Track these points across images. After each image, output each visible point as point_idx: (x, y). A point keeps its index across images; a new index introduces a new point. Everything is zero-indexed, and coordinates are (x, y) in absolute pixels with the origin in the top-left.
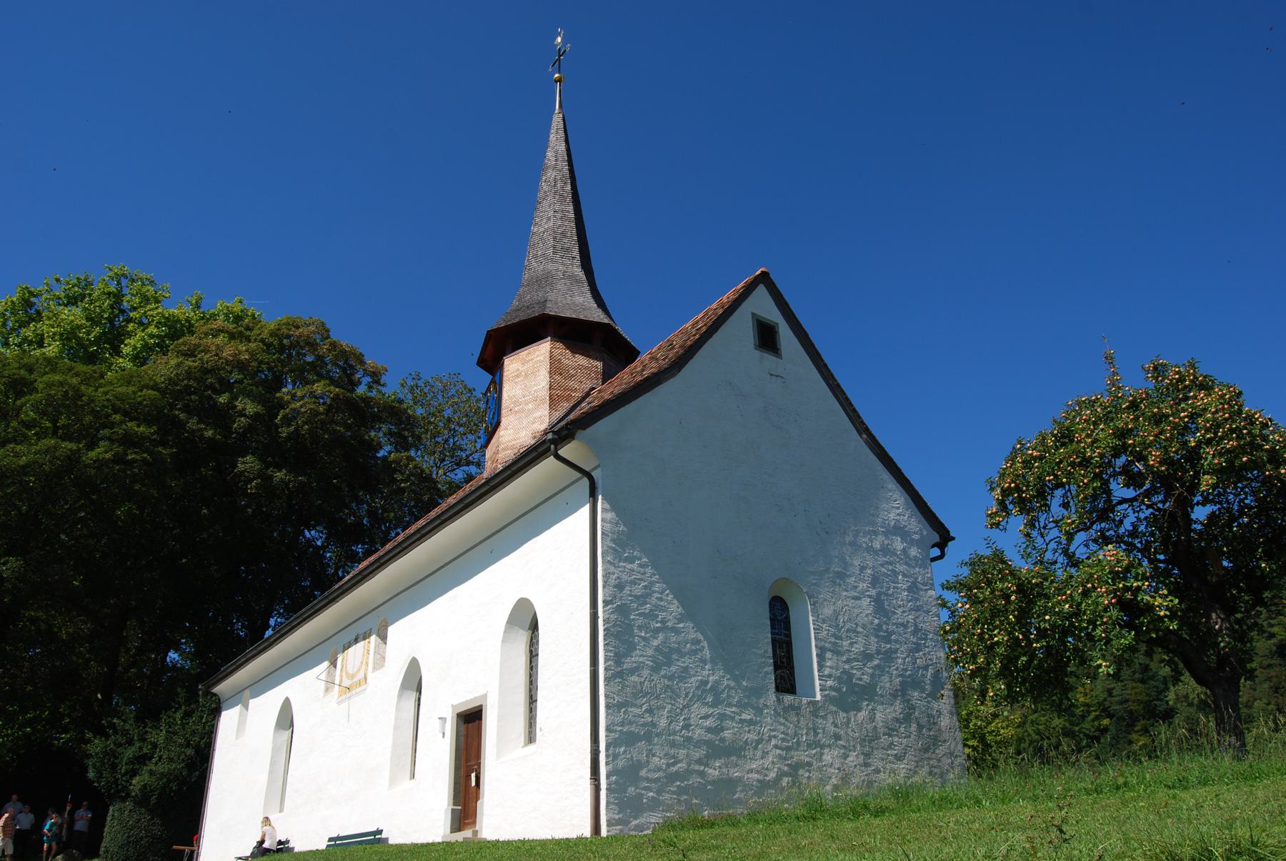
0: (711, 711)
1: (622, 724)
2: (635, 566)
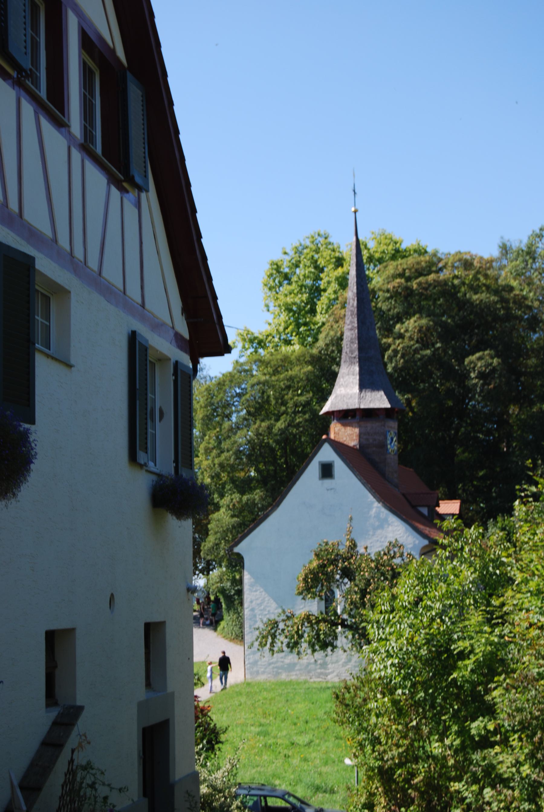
2: (258, 593)
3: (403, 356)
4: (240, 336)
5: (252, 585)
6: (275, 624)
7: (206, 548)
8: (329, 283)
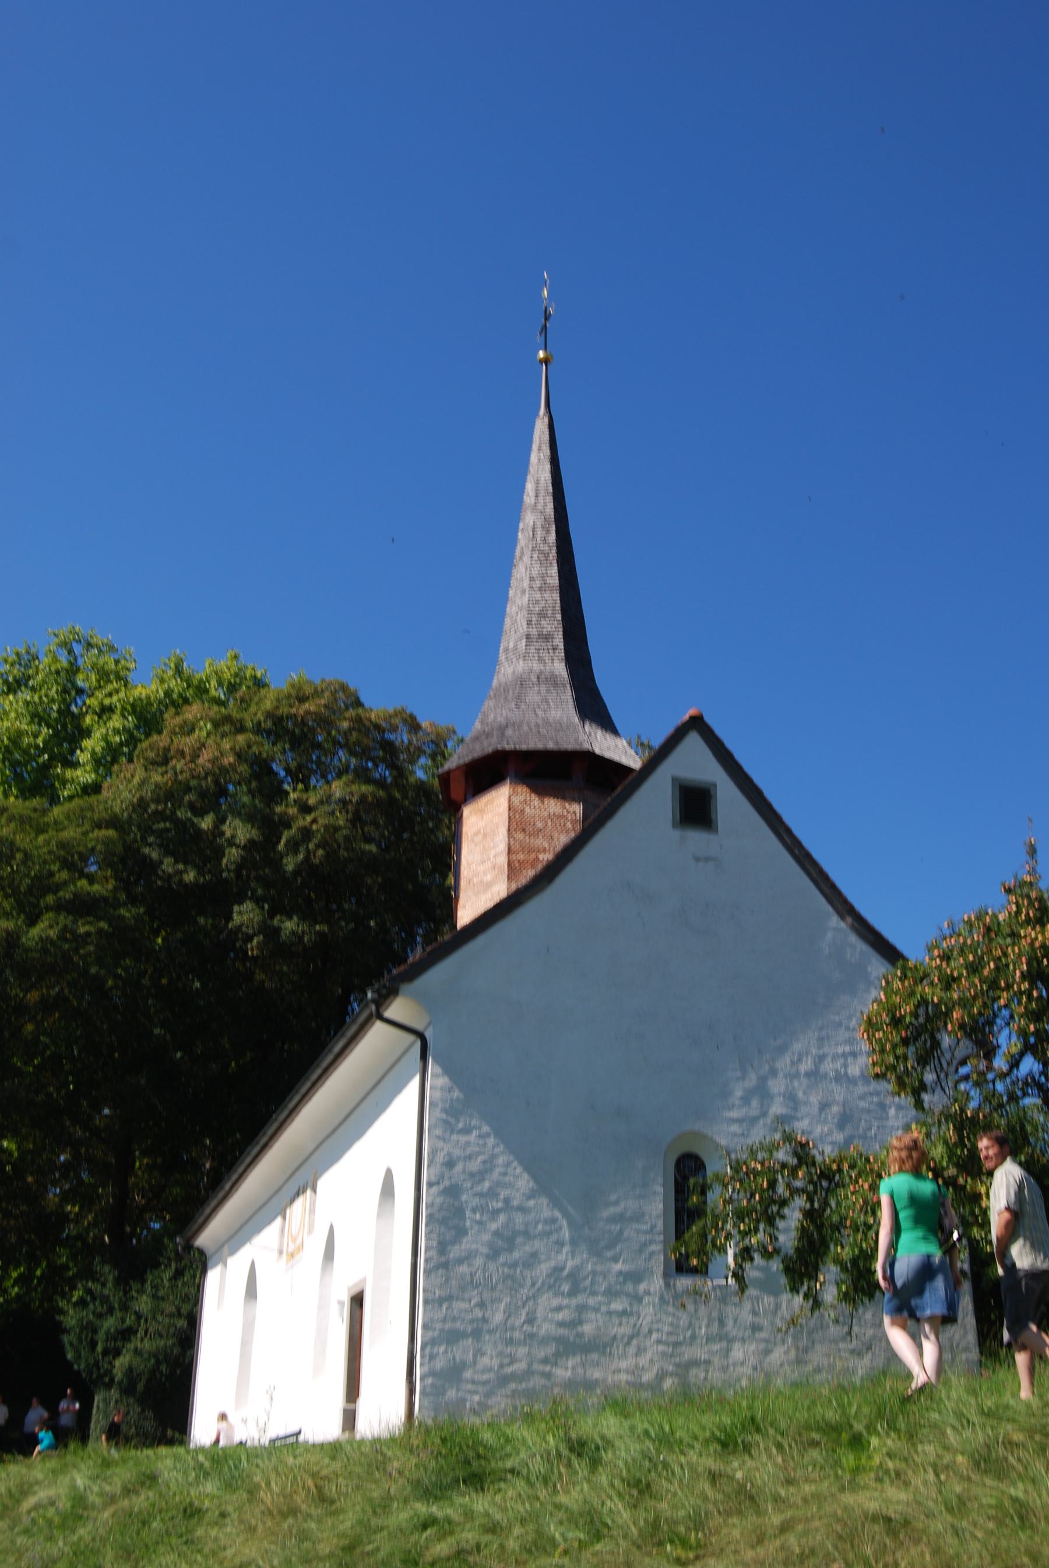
0: (566, 1302)
1: (444, 1320)
2: (472, 1137)
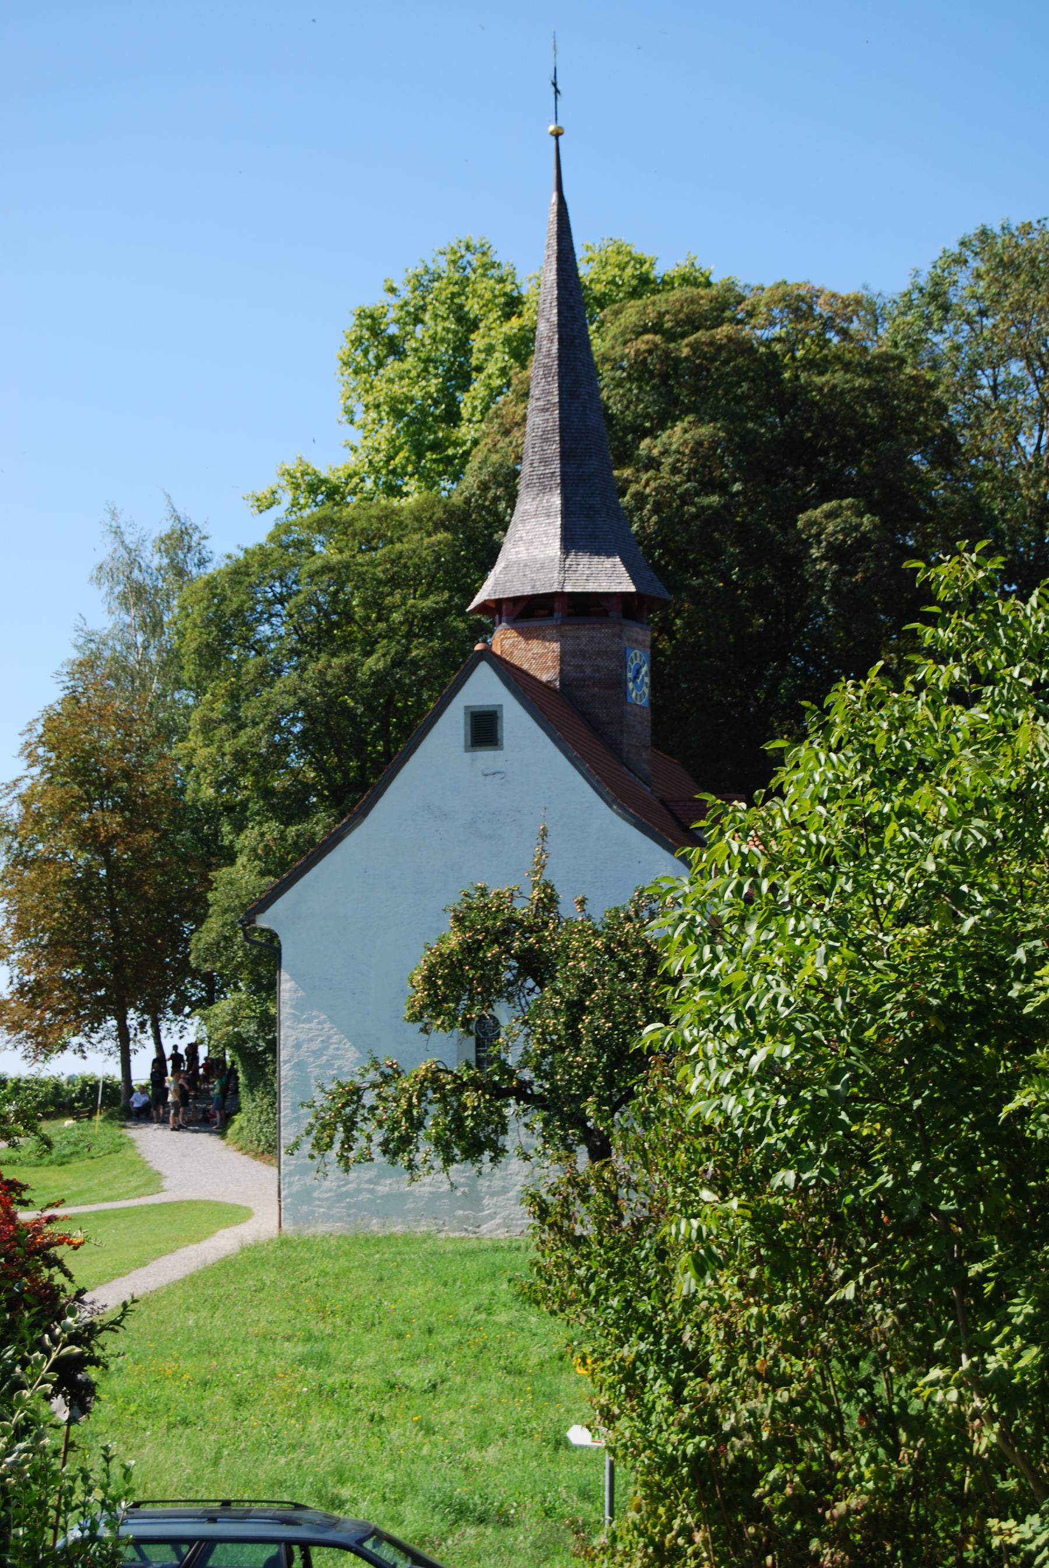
2: (313, 1025)
3: (657, 509)
4: (287, 477)
5: (300, 1006)
6: (357, 1092)
7: (201, 945)
8: (490, 350)
